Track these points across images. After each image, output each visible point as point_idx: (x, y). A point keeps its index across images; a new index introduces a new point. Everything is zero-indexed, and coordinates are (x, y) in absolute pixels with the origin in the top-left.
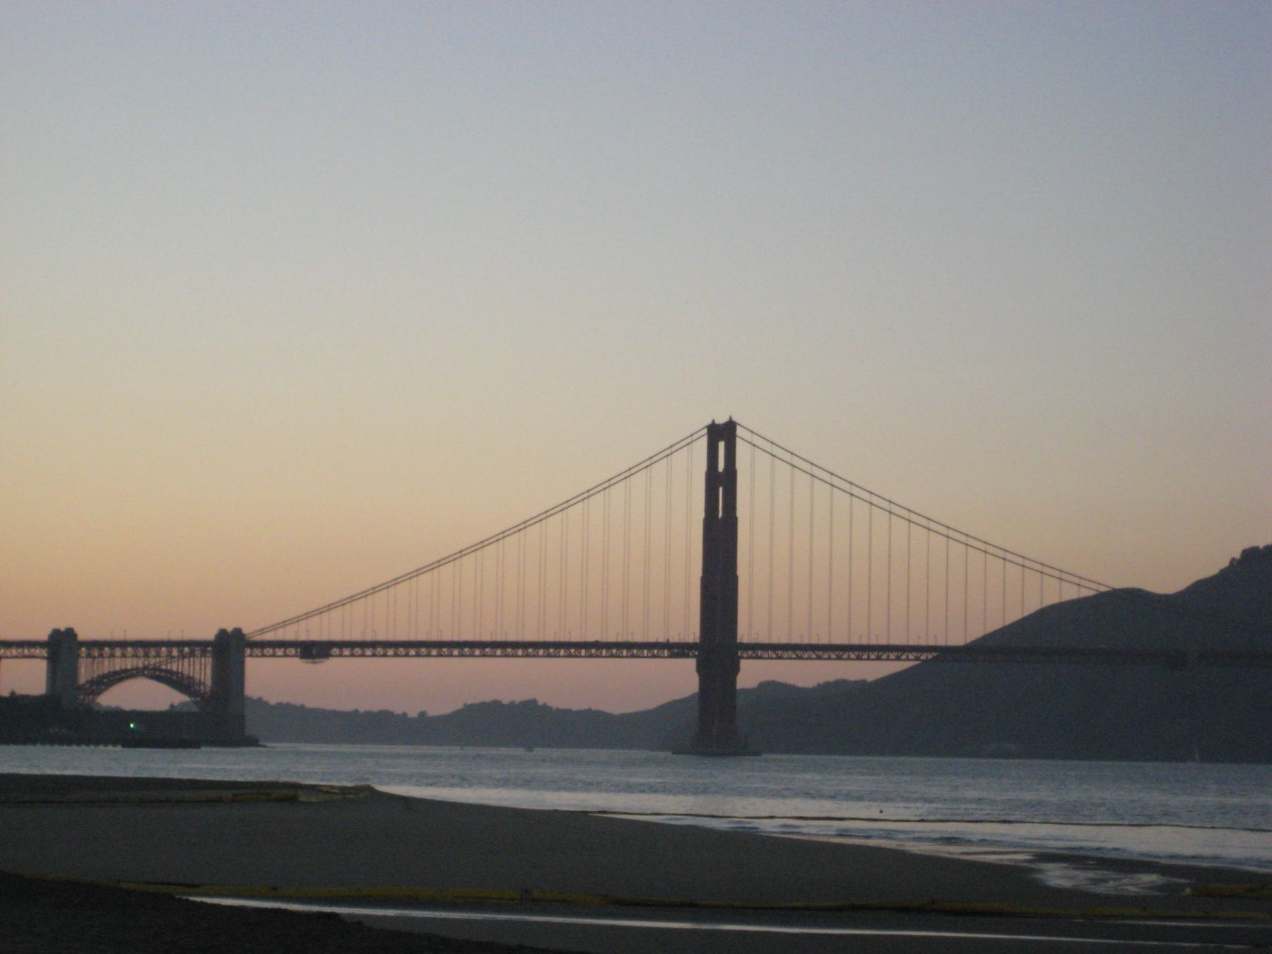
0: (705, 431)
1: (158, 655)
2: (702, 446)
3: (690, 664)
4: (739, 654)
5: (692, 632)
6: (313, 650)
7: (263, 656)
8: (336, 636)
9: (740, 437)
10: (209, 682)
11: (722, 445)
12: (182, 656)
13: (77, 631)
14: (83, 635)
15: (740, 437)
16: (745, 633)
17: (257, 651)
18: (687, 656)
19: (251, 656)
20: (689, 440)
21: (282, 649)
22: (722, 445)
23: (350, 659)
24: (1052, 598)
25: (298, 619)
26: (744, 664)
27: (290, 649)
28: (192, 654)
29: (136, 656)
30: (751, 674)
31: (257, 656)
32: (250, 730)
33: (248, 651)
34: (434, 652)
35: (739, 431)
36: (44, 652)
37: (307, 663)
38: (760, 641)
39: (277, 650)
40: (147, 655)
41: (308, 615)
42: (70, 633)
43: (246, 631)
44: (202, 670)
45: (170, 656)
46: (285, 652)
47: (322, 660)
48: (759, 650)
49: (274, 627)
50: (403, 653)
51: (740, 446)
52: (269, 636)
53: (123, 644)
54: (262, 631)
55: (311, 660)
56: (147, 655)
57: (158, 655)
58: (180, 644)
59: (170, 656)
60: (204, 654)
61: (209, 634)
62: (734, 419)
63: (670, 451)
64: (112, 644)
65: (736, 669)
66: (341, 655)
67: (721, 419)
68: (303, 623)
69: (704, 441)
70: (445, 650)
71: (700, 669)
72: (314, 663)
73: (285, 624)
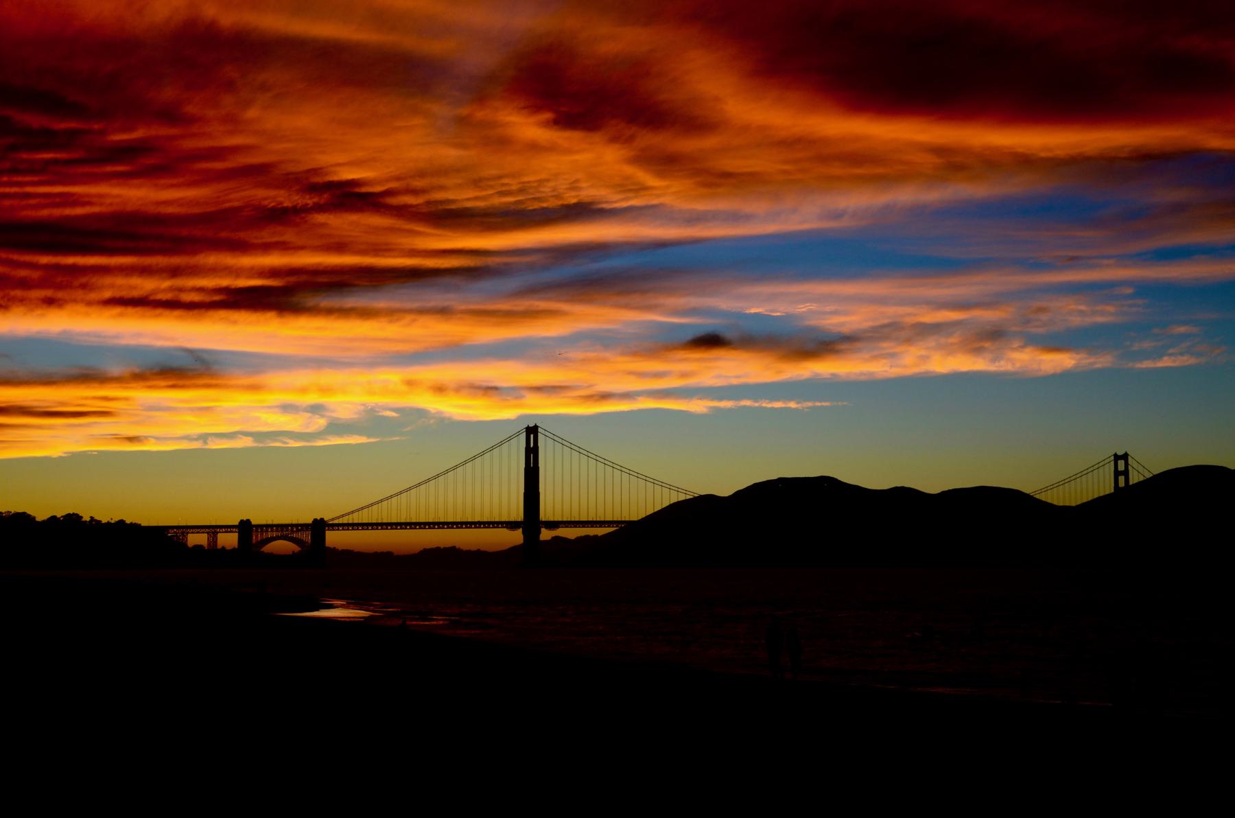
1: (287, 530)
2: (523, 437)
7: (334, 530)
10: (310, 542)
11: (532, 436)
12: (298, 531)
13: (251, 520)
14: (254, 522)
16: (543, 517)
19: (328, 530)
20: (518, 434)
22: (532, 436)
24: (674, 500)
25: (348, 514)
28: (300, 530)
29: (277, 531)
30: (546, 535)
35: (540, 430)
36: (237, 530)
40: (282, 531)
41: (353, 512)
42: (248, 521)
43: (325, 519)
44: (307, 537)
45: (292, 530)
49: (338, 518)
51: (540, 437)
52: (336, 522)
53: (271, 526)
54: (333, 519)
56: (282, 531)
57: (287, 530)
58: (297, 525)
59: (292, 530)
60: (307, 530)
61: (310, 521)
63: (510, 439)
64: (267, 526)
65: (540, 532)
67: (531, 425)
69: (525, 433)
71: (523, 533)
73: (343, 516)
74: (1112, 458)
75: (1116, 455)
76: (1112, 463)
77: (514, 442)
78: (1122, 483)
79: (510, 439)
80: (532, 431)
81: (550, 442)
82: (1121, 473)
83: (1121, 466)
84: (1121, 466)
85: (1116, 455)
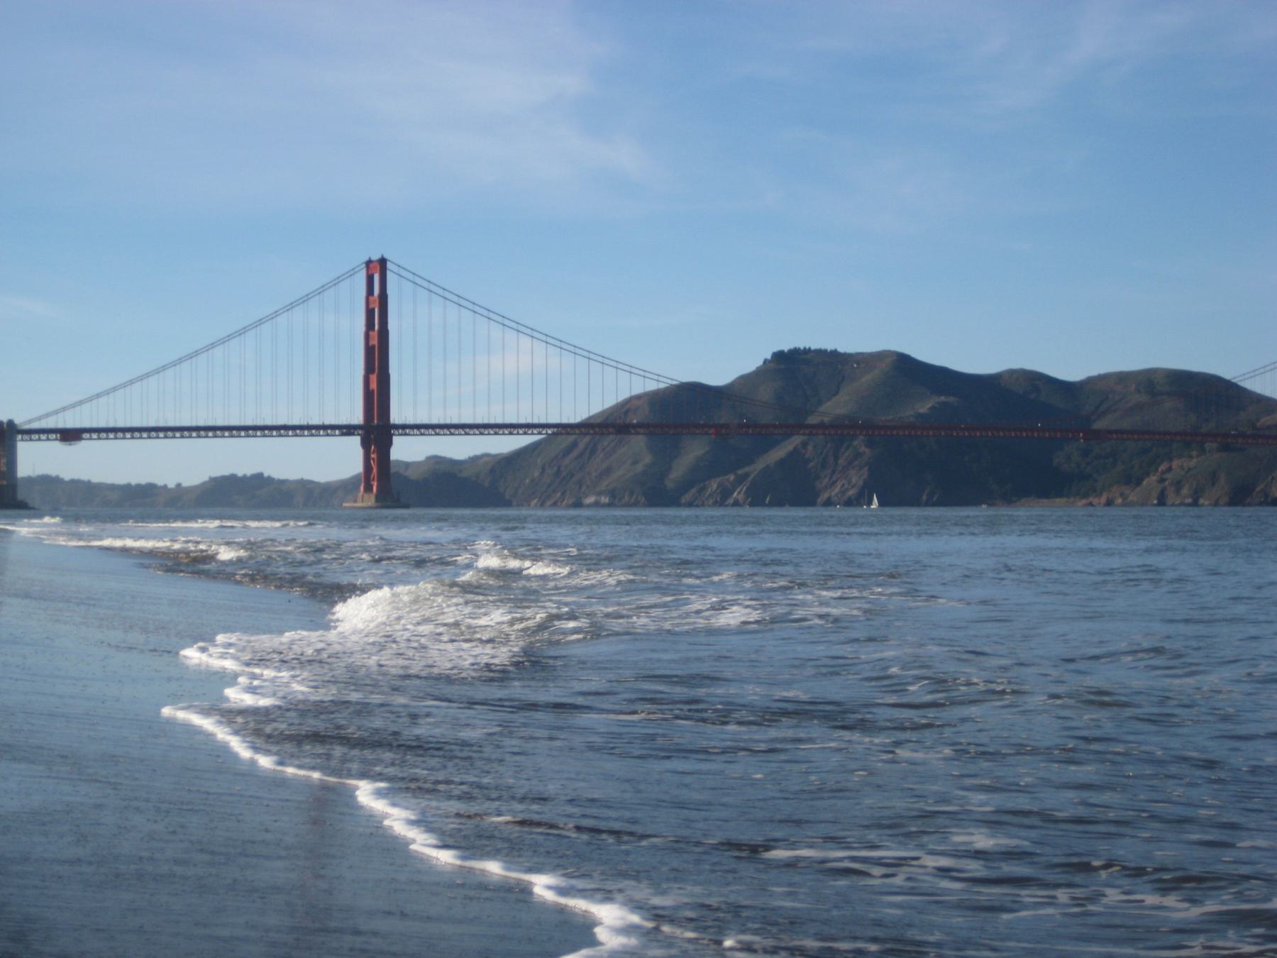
0: (364, 265)
3: (355, 442)
4: (392, 432)
5: (357, 417)
6: (70, 435)
7: (31, 440)
8: (87, 425)
9: (391, 271)
15: (391, 271)
16: (396, 417)
17: (26, 437)
18: (353, 434)
19: (22, 440)
20: (352, 273)
21: (46, 435)
23: (97, 441)
25: (56, 412)
26: (396, 440)
27: (103, 434)
31: (26, 440)
32: (21, 495)
33: (19, 437)
34: (178, 434)
35: (389, 265)
37: (65, 445)
38: (408, 423)
39: (41, 435)
41: (64, 409)
43: (19, 420)
46: (39, 437)
47: (76, 442)
48: (405, 428)
49: (39, 419)
50: (155, 435)
52: (35, 425)
54: (30, 421)
55: (68, 443)
62: (386, 256)
63: (337, 281)
65: (390, 443)
66: (91, 439)
67: (375, 257)
68: (61, 415)
69: (364, 271)
70: (234, 432)
71: (365, 444)
72: (71, 445)
73: (47, 415)
77: (345, 285)
79: (337, 281)
80: (378, 268)
81: (408, 286)
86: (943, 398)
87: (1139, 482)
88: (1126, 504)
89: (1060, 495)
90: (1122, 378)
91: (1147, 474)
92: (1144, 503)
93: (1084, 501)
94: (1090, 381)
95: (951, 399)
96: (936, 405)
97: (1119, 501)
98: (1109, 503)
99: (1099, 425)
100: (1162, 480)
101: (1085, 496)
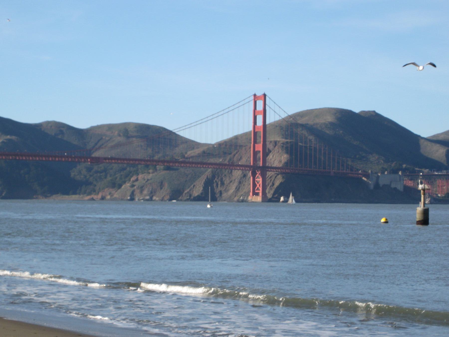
74: (252, 98)
75: (255, 95)
76: (252, 103)
78: (260, 123)
82: (259, 113)
83: (260, 106)
84: (260, 106)
85: (255, 95)
86: (9, 137)
87: (120, 186)
88: (113, 199)
89: (75, 193)
90: (110, 127)
91: (125, 182)
92: (122, 199)
93: (89, 197)
94: (92, 128)
95: (13, 137)
96: (5, 141)
97: (108, 197)
98: (103, 198)
99: (96, 154)
100: (133, 186)
101: (90, 194)
